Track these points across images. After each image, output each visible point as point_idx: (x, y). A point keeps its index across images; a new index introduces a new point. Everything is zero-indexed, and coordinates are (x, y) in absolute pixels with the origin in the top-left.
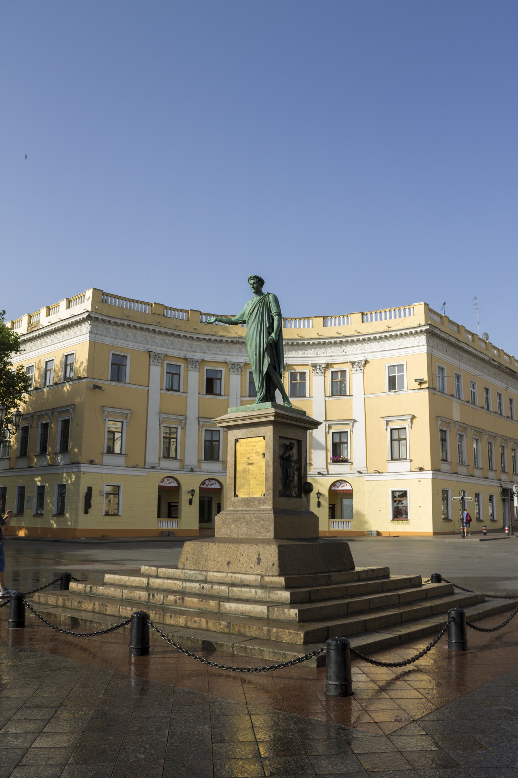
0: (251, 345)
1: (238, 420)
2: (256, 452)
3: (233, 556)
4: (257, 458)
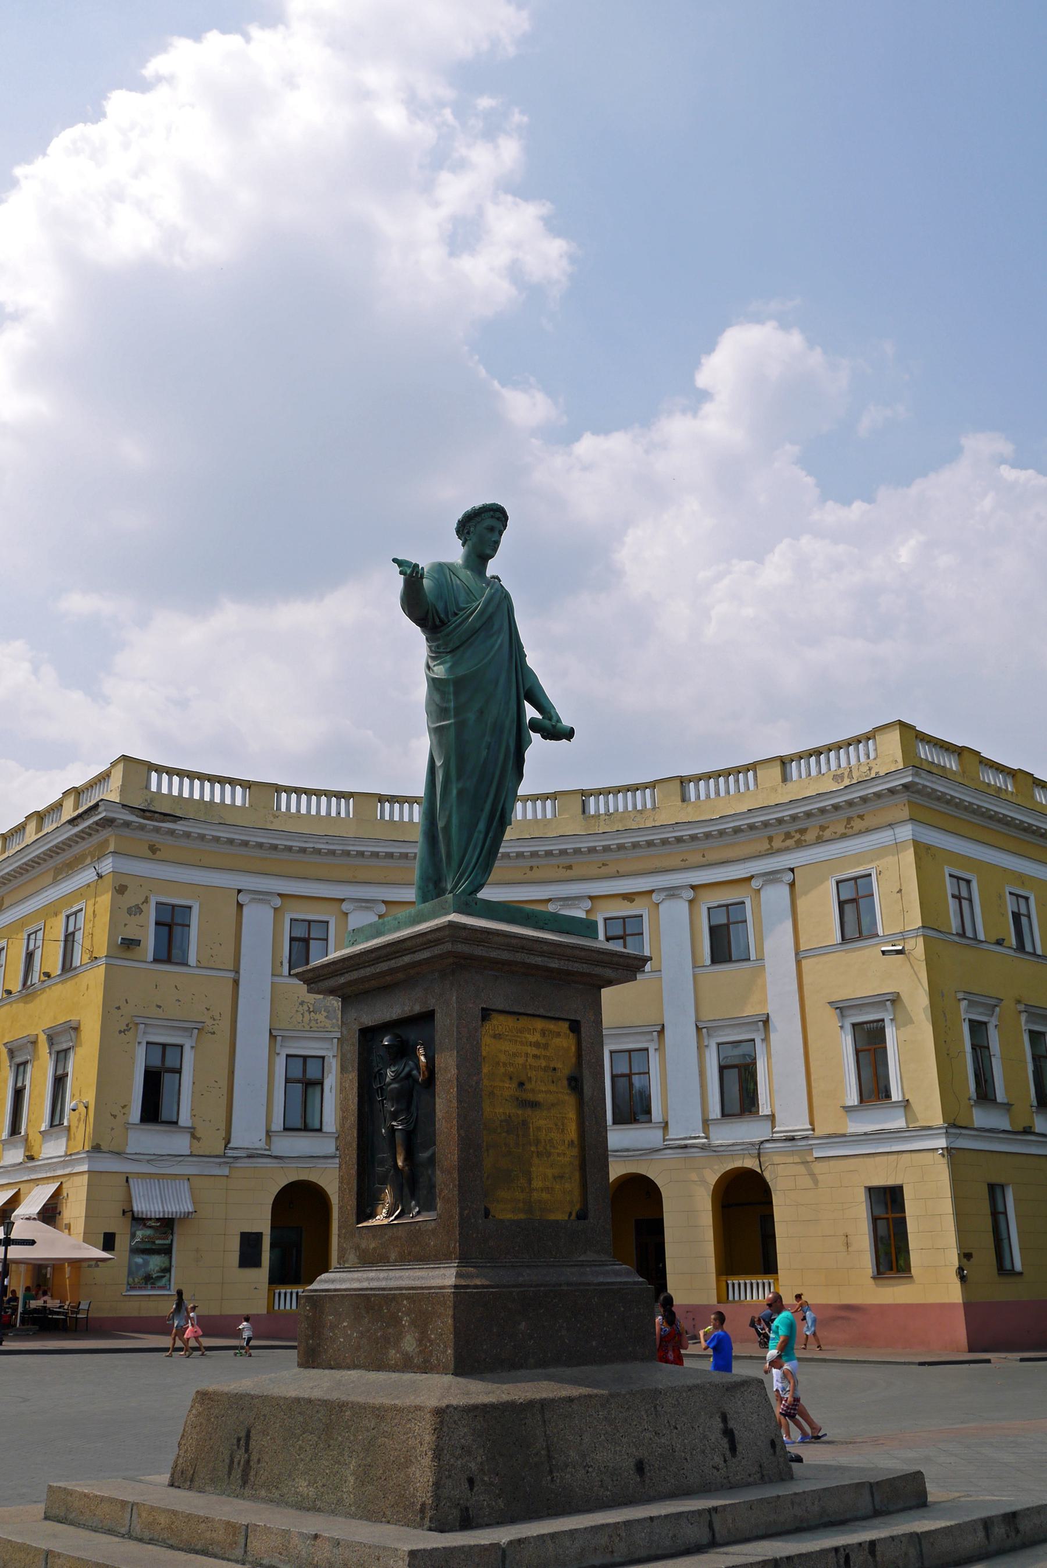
0: (481, 712)
1: (530, 951)
2: (546, 1069)
3: (648, 1435)
4: (553, 1088)
